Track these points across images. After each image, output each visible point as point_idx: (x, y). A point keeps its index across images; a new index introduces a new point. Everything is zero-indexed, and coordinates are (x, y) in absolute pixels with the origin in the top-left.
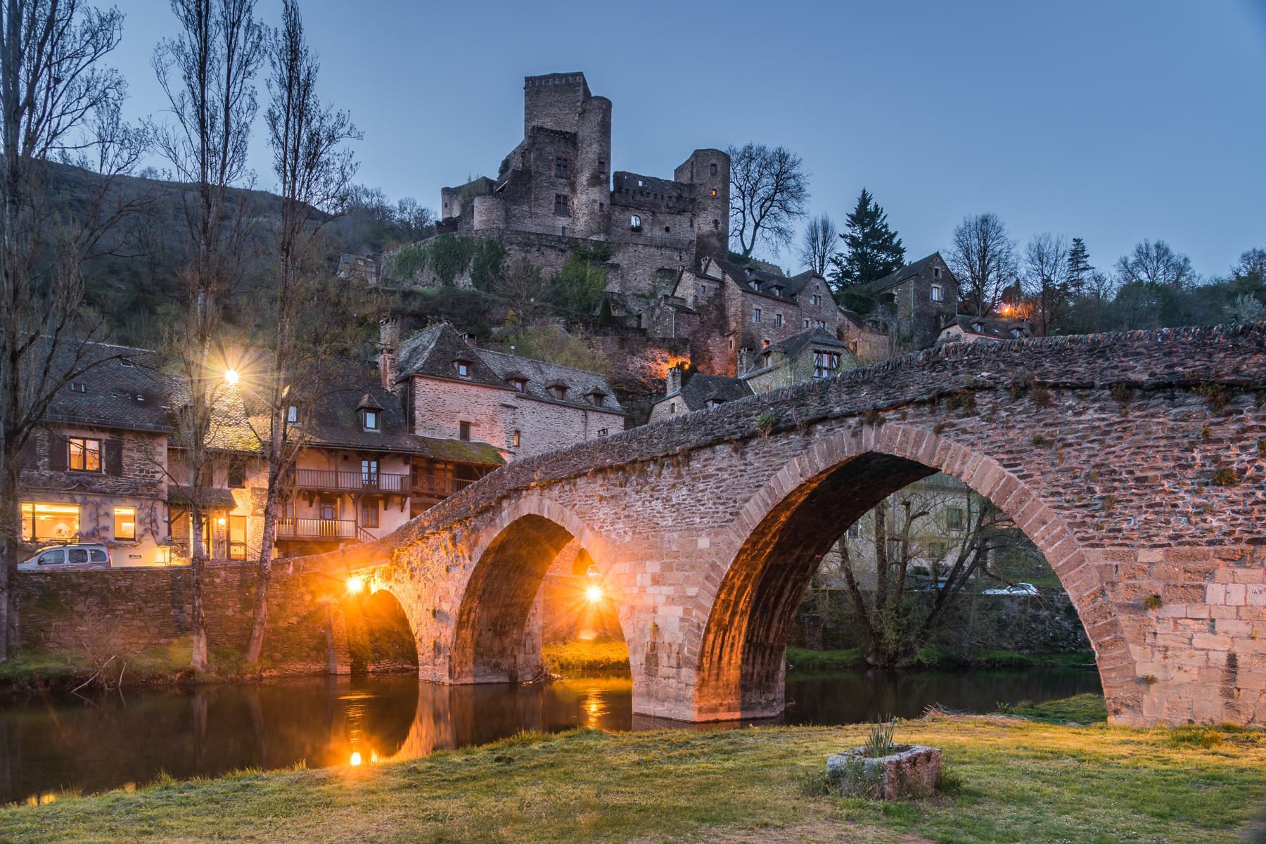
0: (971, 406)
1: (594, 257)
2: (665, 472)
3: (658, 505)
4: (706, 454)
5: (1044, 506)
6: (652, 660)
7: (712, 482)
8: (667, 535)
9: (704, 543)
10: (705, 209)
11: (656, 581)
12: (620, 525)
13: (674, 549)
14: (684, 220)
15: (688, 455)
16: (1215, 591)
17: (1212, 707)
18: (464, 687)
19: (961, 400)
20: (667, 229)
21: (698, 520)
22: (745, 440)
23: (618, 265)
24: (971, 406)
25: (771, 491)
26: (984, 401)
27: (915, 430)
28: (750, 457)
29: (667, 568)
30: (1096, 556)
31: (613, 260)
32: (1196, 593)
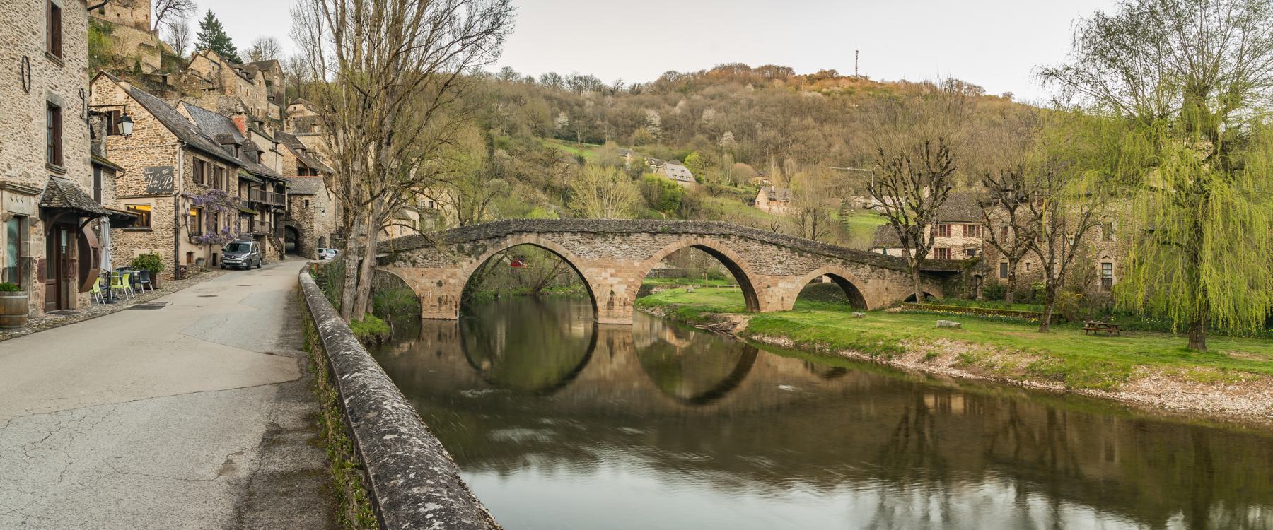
0: (729, 239)
1: (104, 30)
2: (616, 238)
3: (614, 249)
4: (638, 235)
5: (747, 264)
6: (610, 304)
7: (640, 245)
8: (619, 260)
9: (636, 264)
10: (140, 7)
11: (612, 275)
12: (592, 254)
13: (622, 265)
14: (128, 11)
15: (629, 234)
16: (779, 284)
17: (780, 308)
18: (444, 322)
19: (727, 236)
20: (118, 15)
21: (633, 256)
22: (655, 234)
23: (118, 39)
24: (729, 239)
25: (665, 251)
26: (733, 238)
27: (714, 241)
28: (657, 239)
29: (617, 271)
30: (758, 276)
31: (114, 34)
32: (776, 285)
